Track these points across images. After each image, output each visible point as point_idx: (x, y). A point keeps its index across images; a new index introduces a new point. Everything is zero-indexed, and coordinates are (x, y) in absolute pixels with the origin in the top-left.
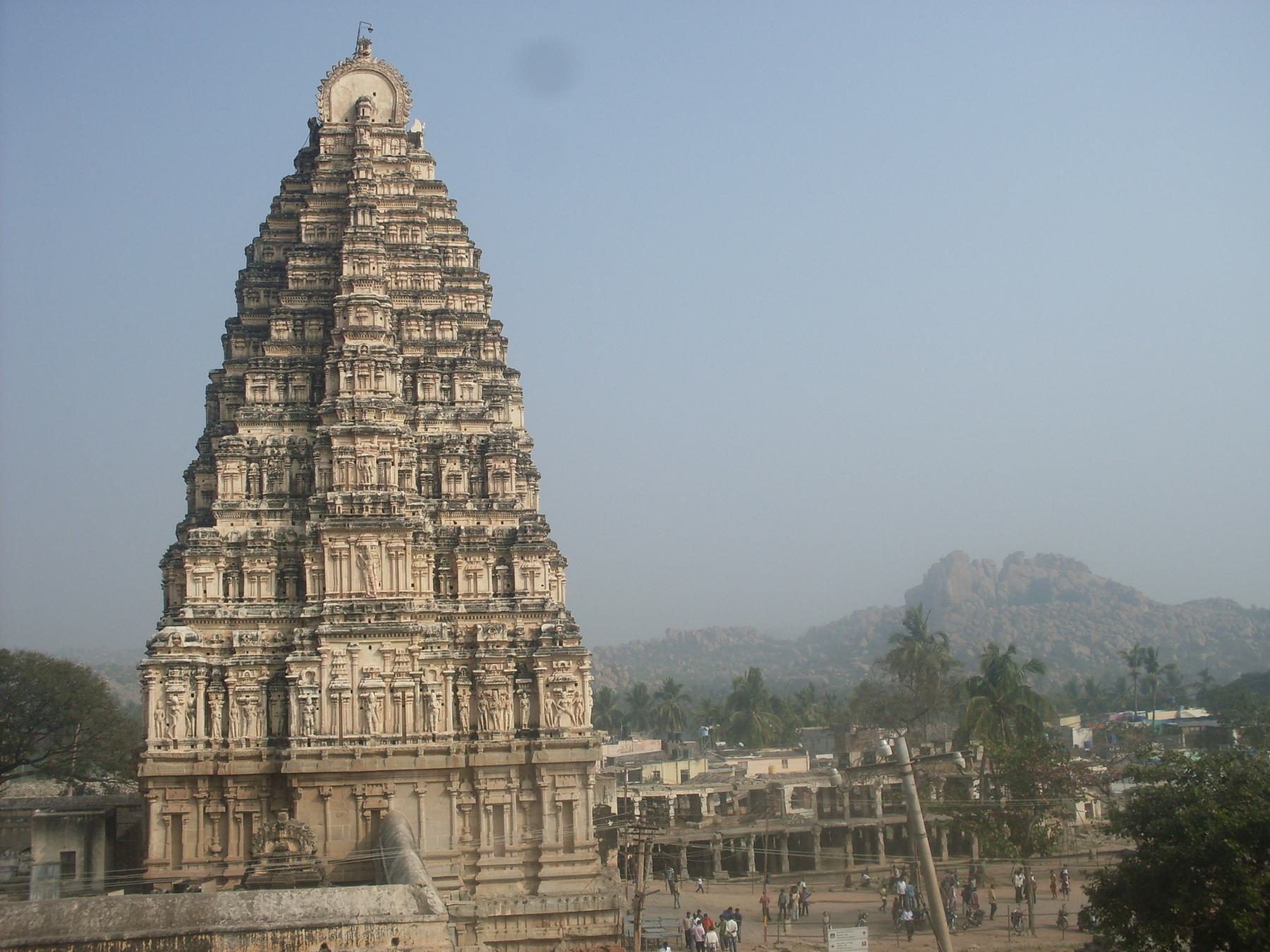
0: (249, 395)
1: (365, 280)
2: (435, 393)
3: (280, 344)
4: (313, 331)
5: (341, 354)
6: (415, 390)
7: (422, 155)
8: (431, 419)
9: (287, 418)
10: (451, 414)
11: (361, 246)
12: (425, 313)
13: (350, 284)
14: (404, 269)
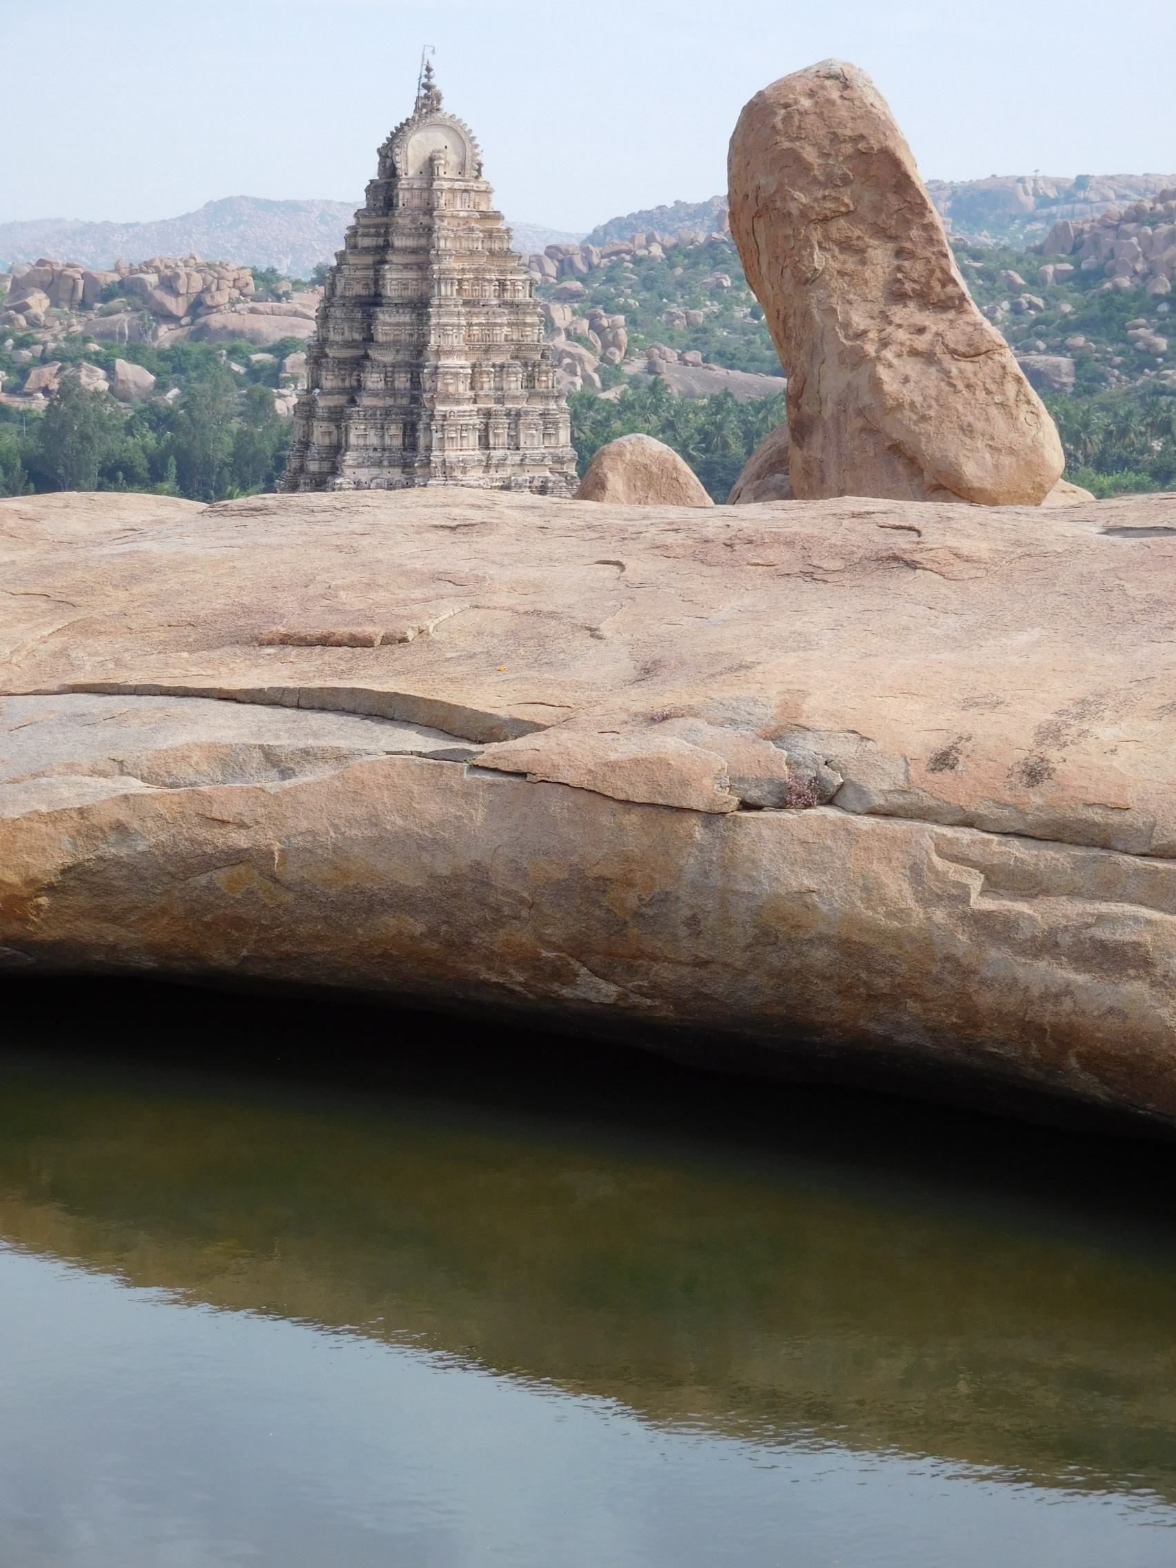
0: (353, 440)
1: (450, 352)
2: (504, 439)
3: (375, 394)
4: (402, 382)
5: (432, 417)
6: (487, 437)
7: (483, 187)
8: (501, 464)
9: (385, 463)
10: (518, 458)
11: (444, 320)
12: (494, 366)
13: (438, 353)
14: (476, 325)
